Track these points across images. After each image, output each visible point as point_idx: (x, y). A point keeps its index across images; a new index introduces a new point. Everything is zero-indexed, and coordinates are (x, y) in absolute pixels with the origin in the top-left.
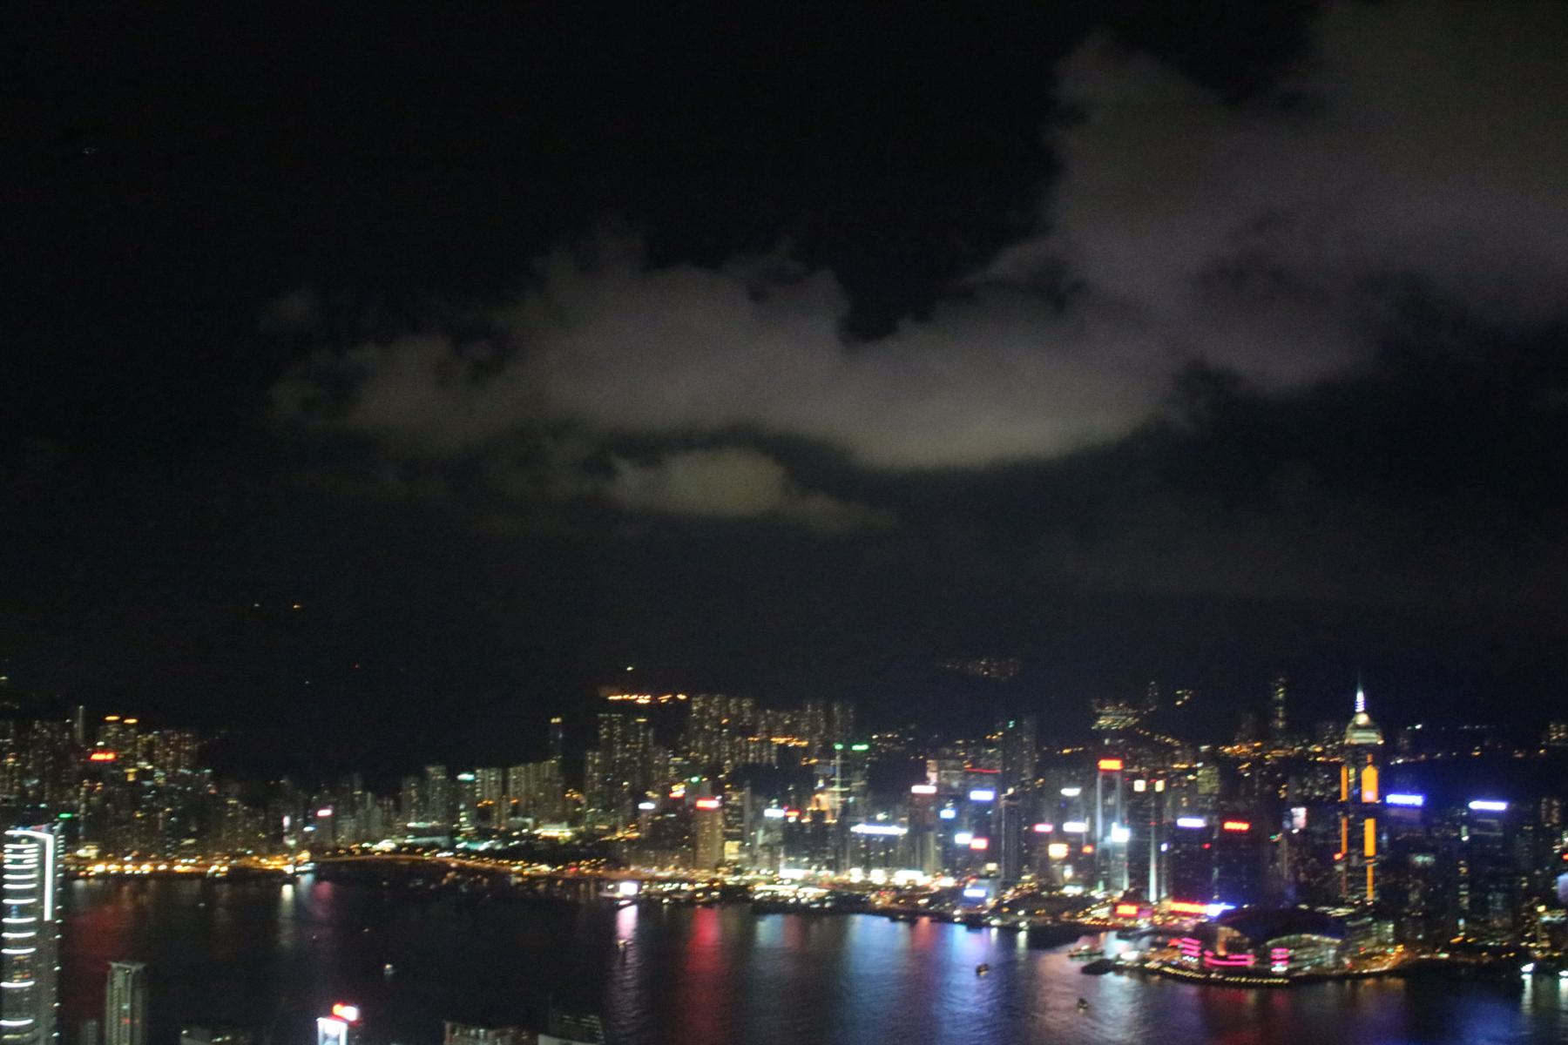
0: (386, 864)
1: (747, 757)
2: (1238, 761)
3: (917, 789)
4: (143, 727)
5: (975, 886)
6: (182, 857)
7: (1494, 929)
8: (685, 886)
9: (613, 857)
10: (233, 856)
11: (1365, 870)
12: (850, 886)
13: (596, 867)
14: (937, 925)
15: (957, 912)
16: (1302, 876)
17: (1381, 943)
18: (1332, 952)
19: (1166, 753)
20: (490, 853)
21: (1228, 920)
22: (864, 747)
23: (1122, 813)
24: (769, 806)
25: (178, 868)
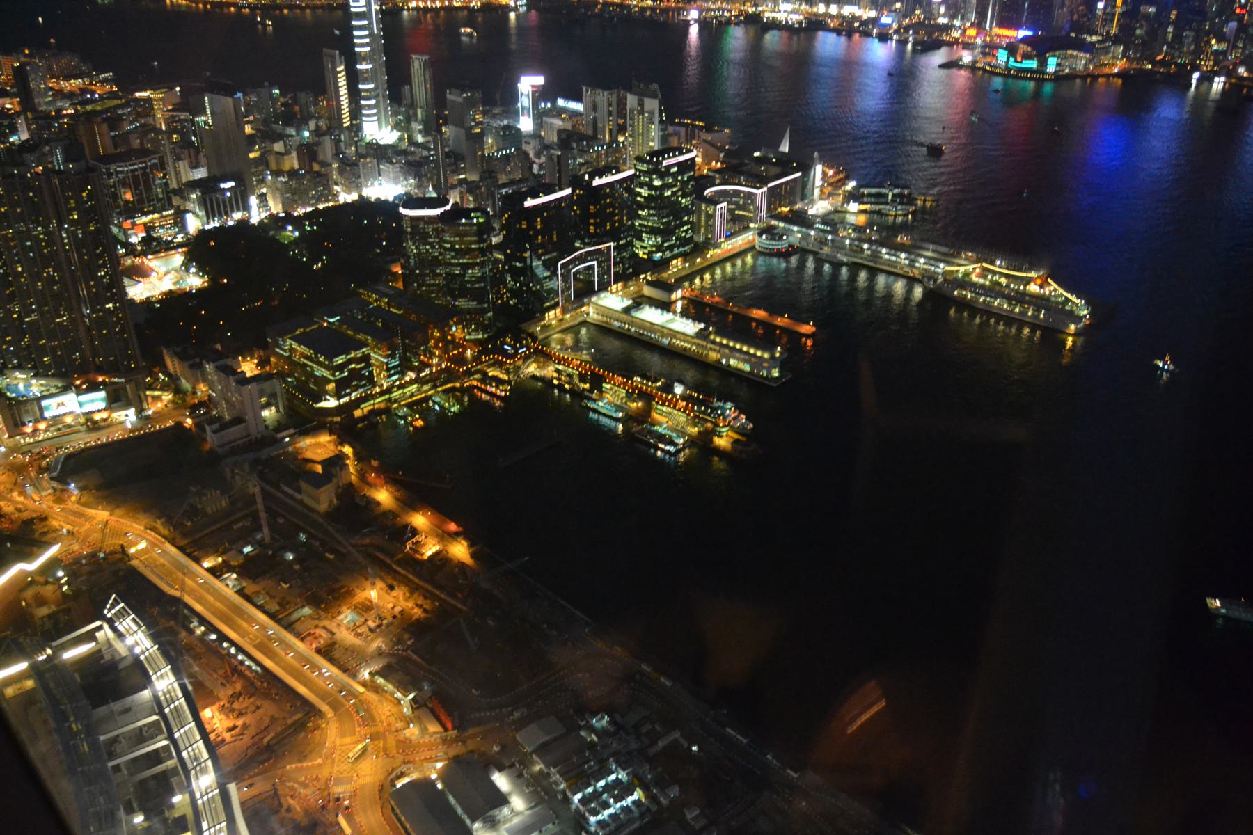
5: (886, 16)
8: (726, 14)
11: (1114, 15)
12: (816, 15)
14: (863, 38)
16: (1075, 17)
17: (1114, 57)
18: (1083, 62)
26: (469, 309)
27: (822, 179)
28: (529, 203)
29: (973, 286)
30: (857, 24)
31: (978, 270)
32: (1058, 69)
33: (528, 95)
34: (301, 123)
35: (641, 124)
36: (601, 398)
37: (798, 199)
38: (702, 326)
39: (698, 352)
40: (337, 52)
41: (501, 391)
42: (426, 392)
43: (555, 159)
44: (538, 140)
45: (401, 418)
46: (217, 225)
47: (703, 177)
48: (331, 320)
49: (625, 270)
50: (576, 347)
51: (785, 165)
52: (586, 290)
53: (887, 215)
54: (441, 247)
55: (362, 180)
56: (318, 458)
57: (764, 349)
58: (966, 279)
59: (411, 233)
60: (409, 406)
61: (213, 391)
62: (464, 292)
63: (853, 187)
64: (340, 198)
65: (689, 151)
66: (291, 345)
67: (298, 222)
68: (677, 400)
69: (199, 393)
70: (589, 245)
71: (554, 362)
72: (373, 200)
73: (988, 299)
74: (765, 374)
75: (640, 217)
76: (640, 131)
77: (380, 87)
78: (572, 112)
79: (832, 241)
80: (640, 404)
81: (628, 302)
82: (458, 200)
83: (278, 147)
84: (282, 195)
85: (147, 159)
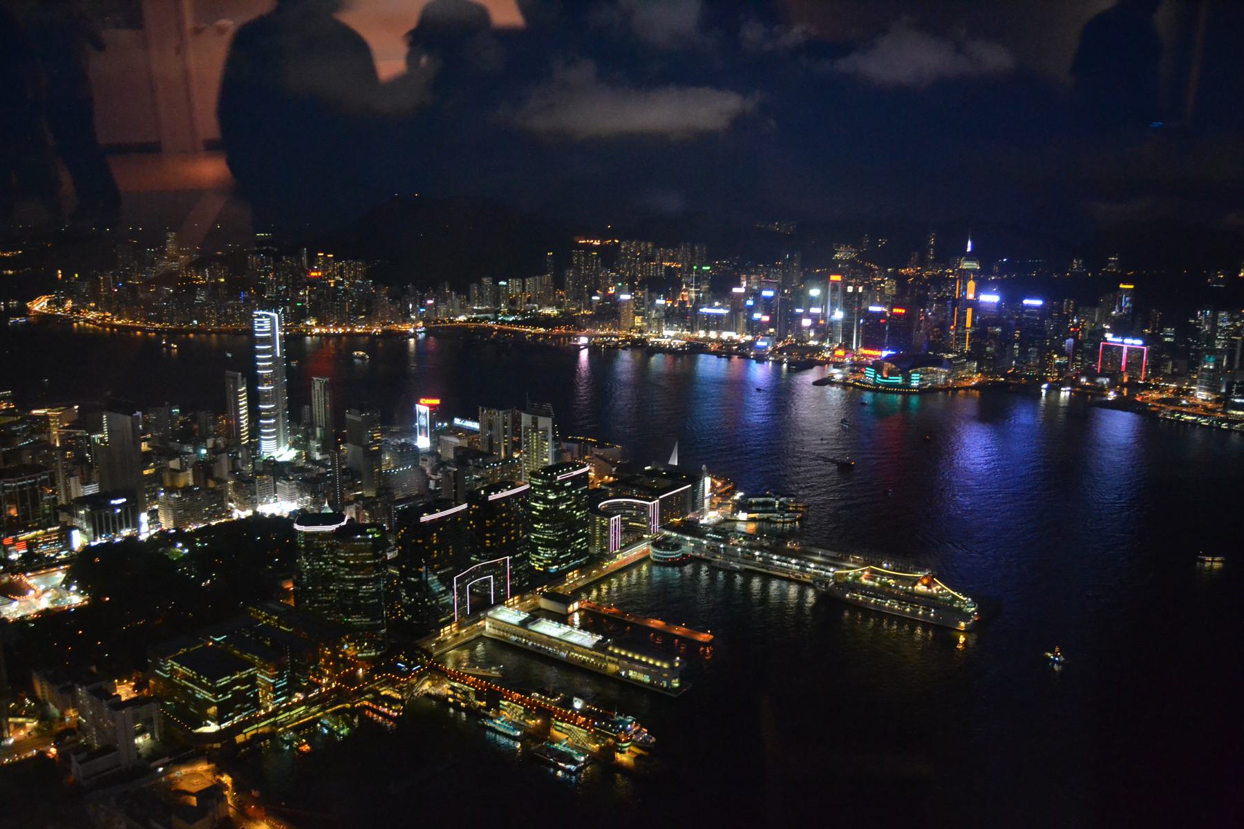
0: (462, 328)
1: (650, 272)
2: (908, 276)
3: (735, 290)
4: (337, 259)
5: (762, 340)
6: (358, 325)
7: (1030, 366)
8: (613, 339)
9: (574, 323)
10: (384, 325)
12: (696, 339)
13: (569, 329)
15: (752, 353)
17: (970, 372)
18: (943, 376)
19: (869, 272)
20: (515, 322)
21: (891, 358)
22: (708, 268)
23: (840, 303)
24: (660, 298)
25: (357, 330)
26: (362, 626)
27: (712, 490)
28: (425, 518)
29: (864, 588)
30: (735, 348)
31: (866, 573)
32: (921, 383)
33: (426, 414)
34: (198, 442)
35: (535, 441)
36: (498, 716)
37: (689, 511)
38: (600, 637)
39: (596, 664)
40: (240, 374)
41: (394, 711)
42: (314, 713)
43: (452, 474)
44: (434, 457)
45: (288, 743)
46: (105, 541)
47: (596, 490)
48: (217, 639)
49: (521, 583)
50: (473, 660)
51: (675, 477)
52: (482, 605)
53: (775, 522)
54: (335, 563)
55: (258, 496)
56: (194, 789)
57: (663, 660)
58: (856, 582)
59: (305, 549)
60: (296, 729)
61: (84, 717)
62: (357, 609)
63: (741, 497)
64: (234, 515)
65: (584, 466)
66: (172, 665)
67: (188, 539)
68: (577, 716)
69: (68, 720)
70: (484, 558)
71: (449, 679)
72: (267, 516)
73: (879, 600)
74: (665, 685)
75: (535, 530)
76: (535, 447)
77: (280, 406)
78: (469, 430)
79: (724, 548)
80: (539, 721)
81: (524, 616)
82: (354, 516)
83: (174, 464)
84: (174, 511)
85: (37, 475)
